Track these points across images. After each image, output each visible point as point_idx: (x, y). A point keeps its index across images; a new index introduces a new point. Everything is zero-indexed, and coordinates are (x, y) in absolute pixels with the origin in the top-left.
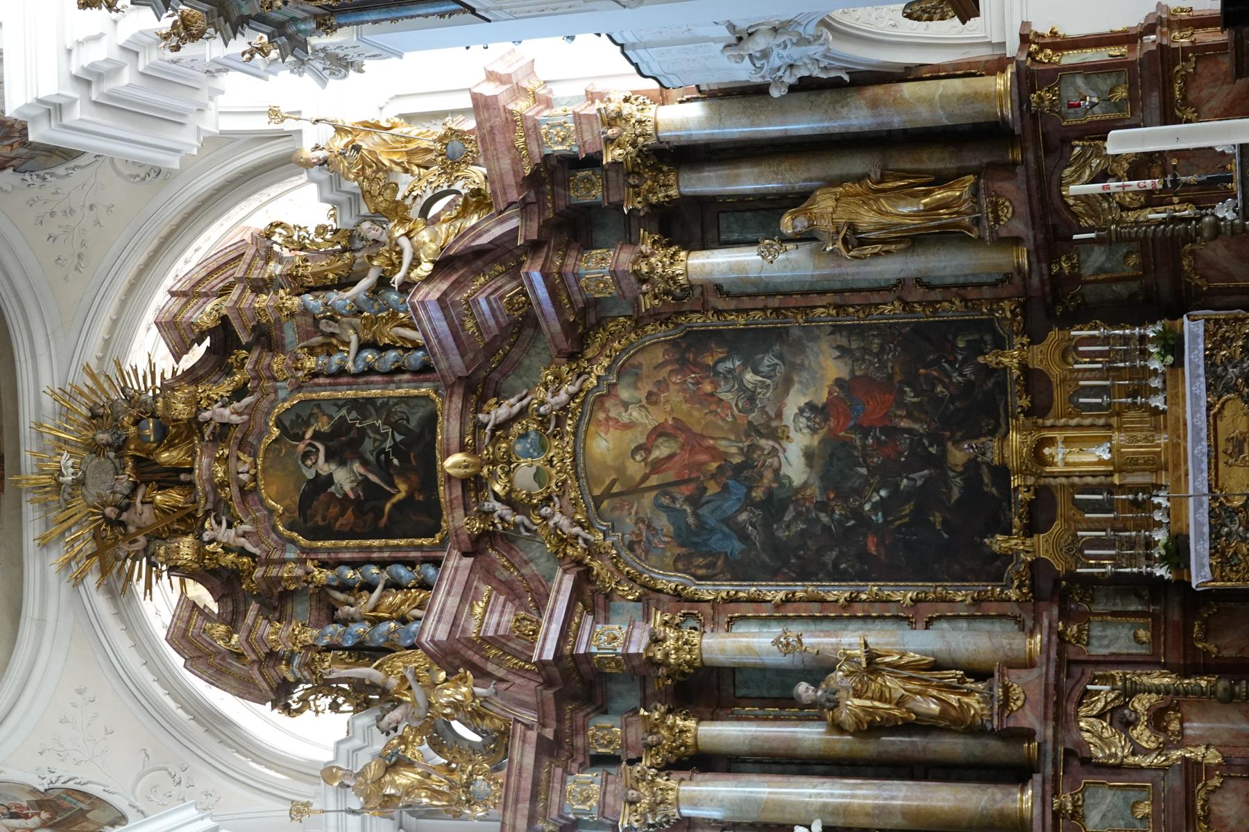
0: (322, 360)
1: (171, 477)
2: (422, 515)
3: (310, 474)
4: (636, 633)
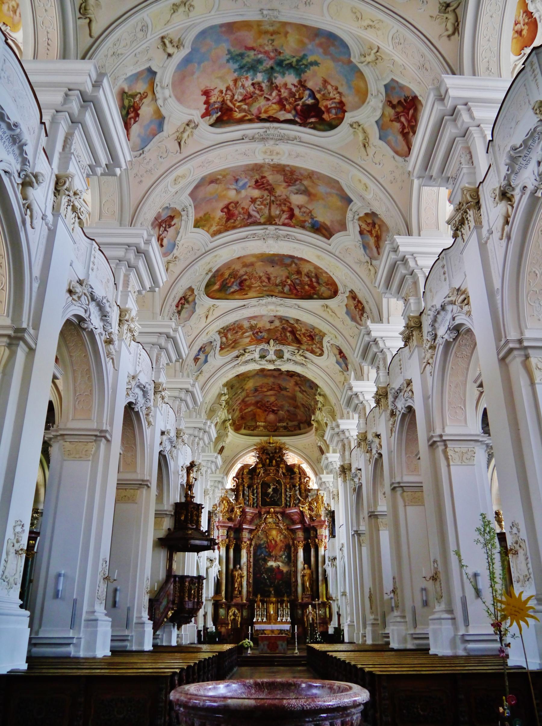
1: (271, 462)
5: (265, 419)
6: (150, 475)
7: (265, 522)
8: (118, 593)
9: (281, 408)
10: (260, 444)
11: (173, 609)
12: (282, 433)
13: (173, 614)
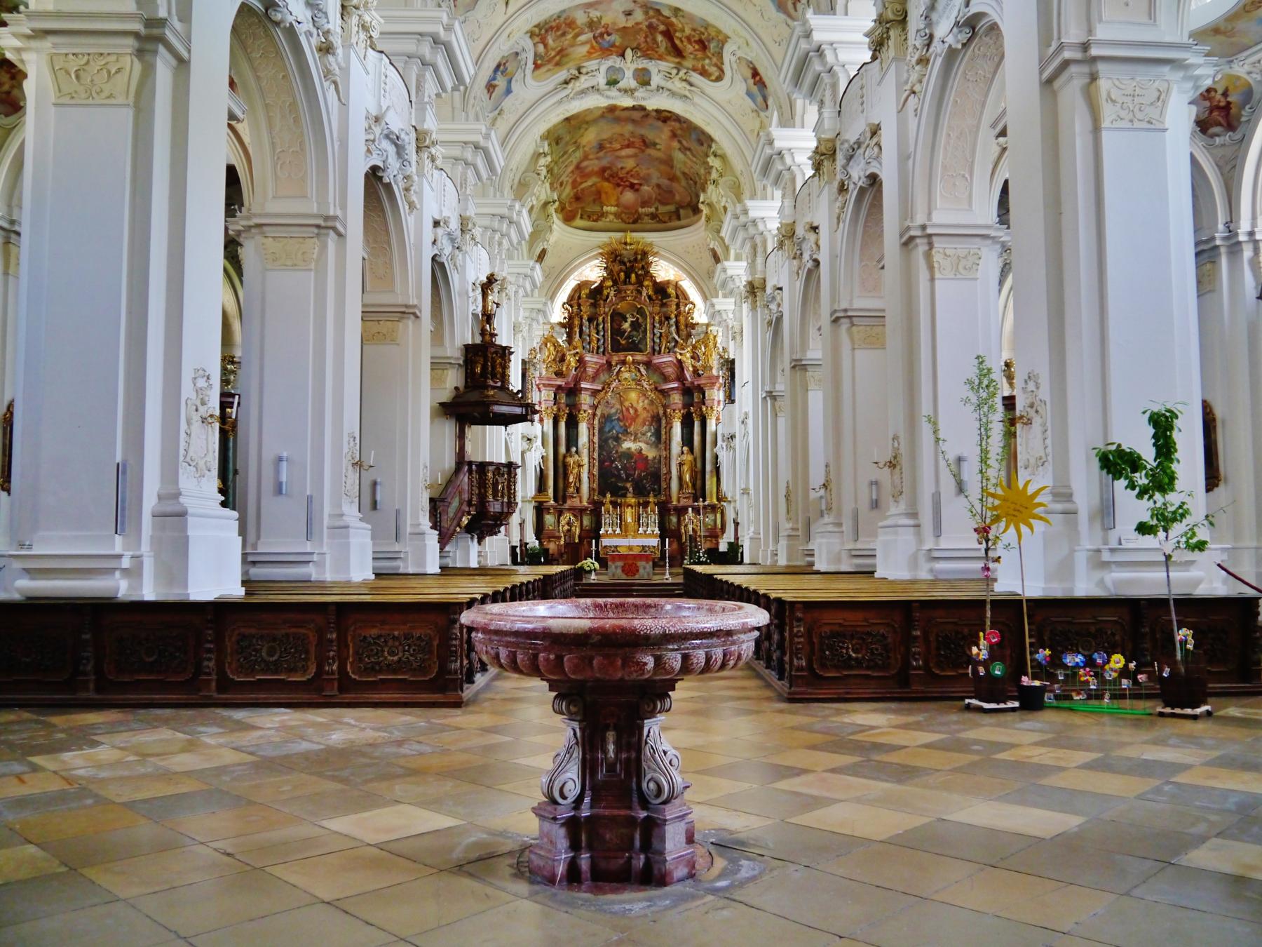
1: (628, 276)
2: (617, 348)
5: (618, 199)
6: (419, 296)
8: (378, 487)
9: (646, 180)
10: (610, 245)
11: (469, 513)
12: (649, 226)
13: (470, 522)
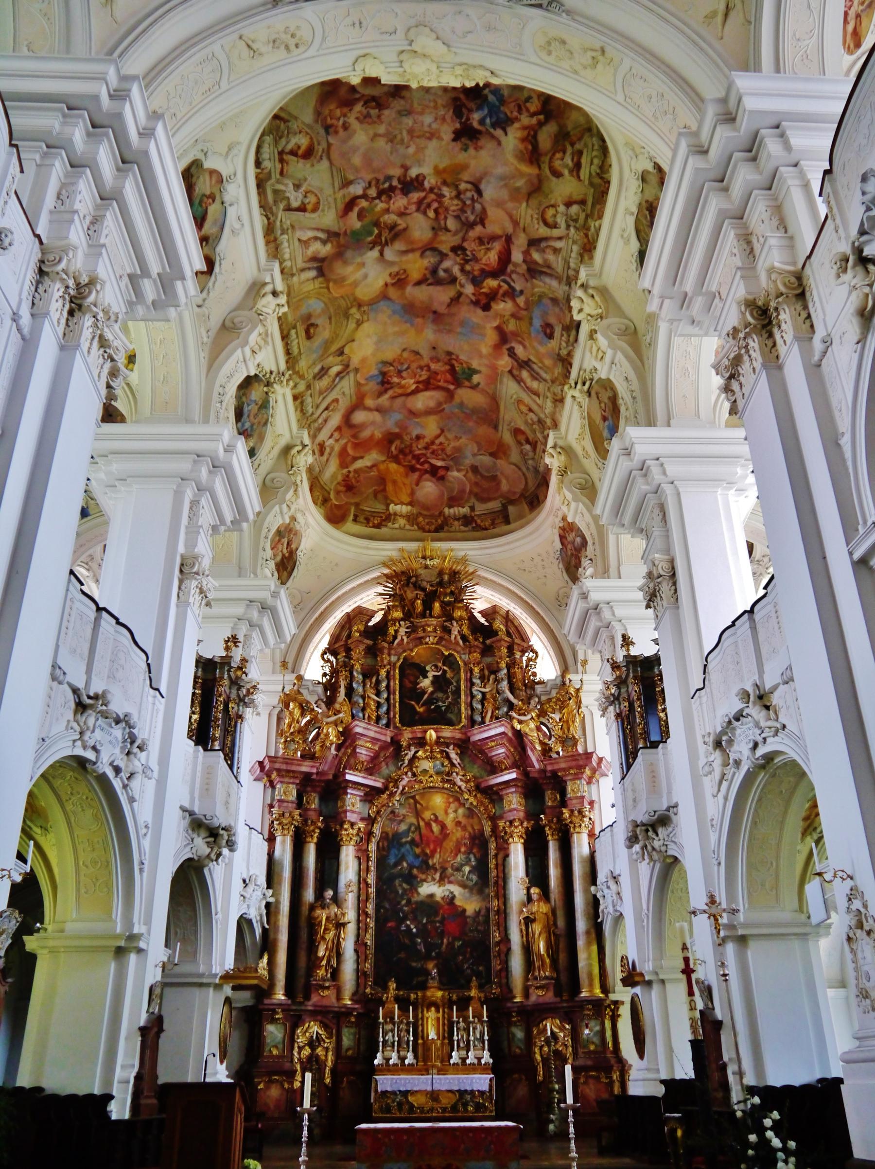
0: (478, 675)
1: (428, 606)
2: (409, 718)
3: (428, 668)
4: (355, 815)
5: (412, 493)
7: (411, 769)
9: (455, 458)
